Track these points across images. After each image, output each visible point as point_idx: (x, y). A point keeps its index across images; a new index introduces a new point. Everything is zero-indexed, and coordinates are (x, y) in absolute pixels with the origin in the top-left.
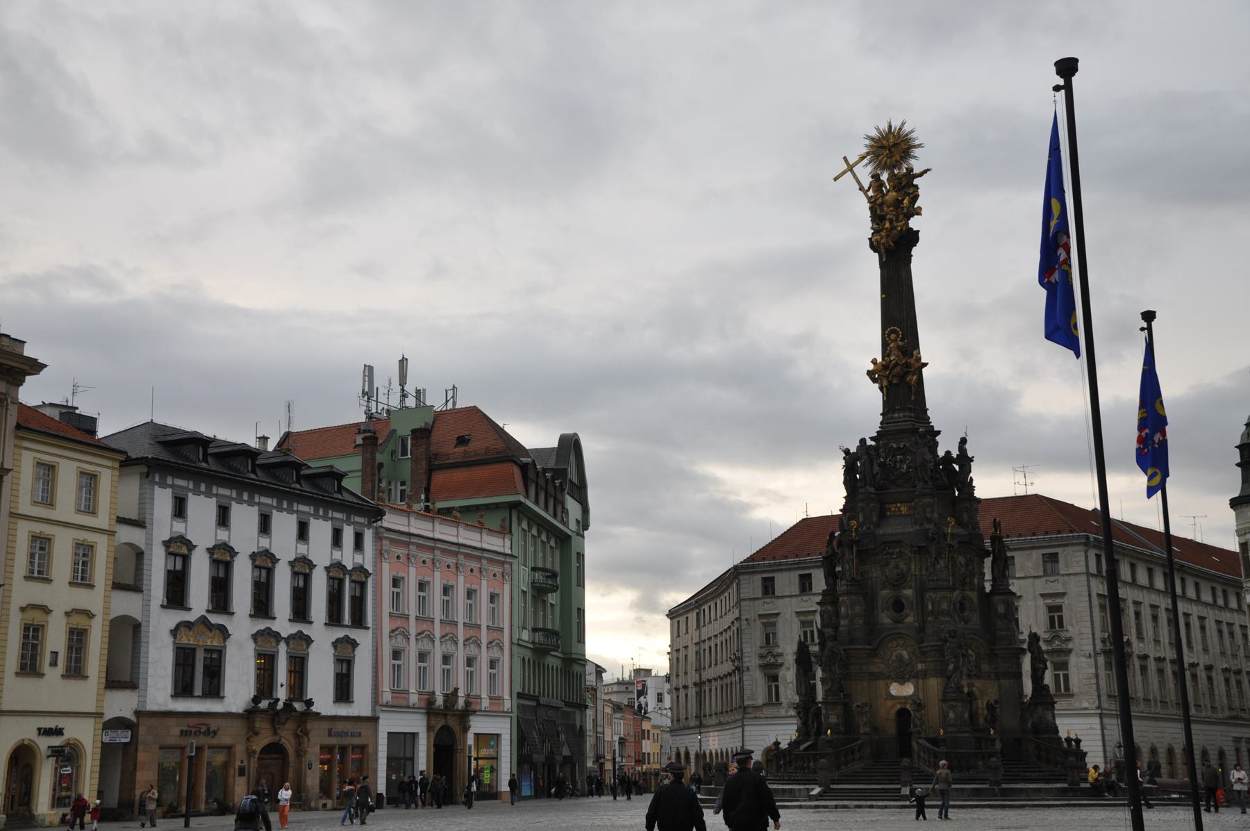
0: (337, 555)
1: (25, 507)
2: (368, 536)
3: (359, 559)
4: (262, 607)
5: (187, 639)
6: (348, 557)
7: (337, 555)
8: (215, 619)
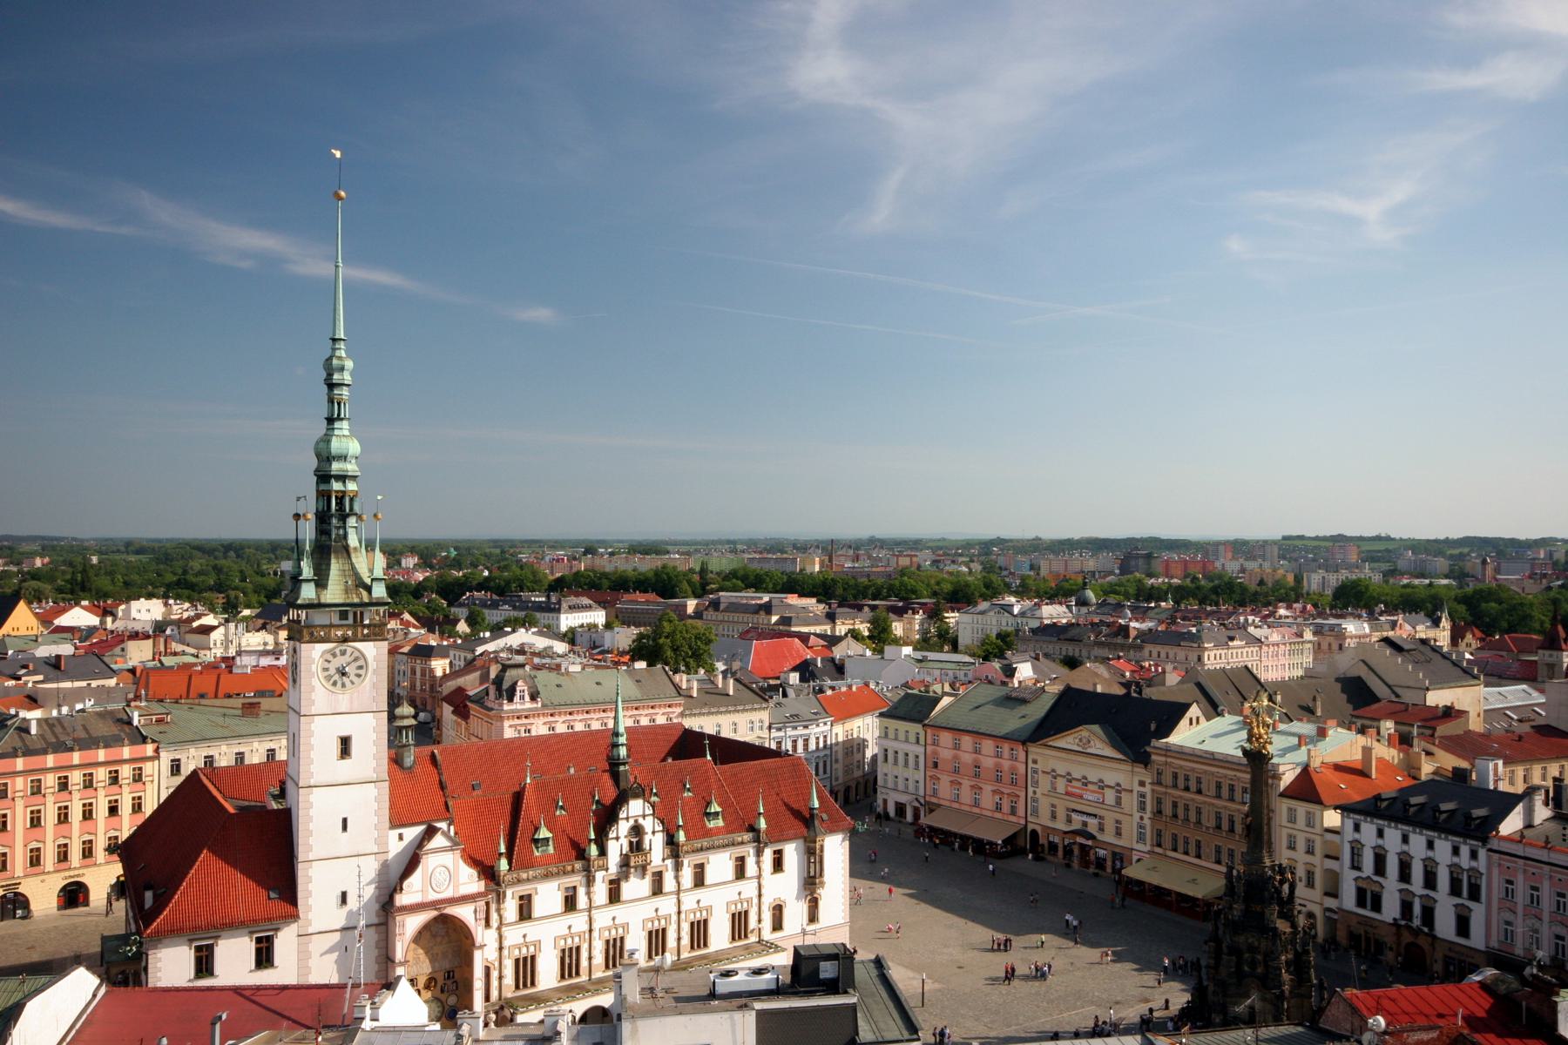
0: (1456, 860)
1: (1285, 823)
2: (1482, 853)
3: (1474, 864)
4: (1405, 875)
5: (1363, 885)
6: (1464, 860)
7: (1456, 860)
8: (1376, 878)
